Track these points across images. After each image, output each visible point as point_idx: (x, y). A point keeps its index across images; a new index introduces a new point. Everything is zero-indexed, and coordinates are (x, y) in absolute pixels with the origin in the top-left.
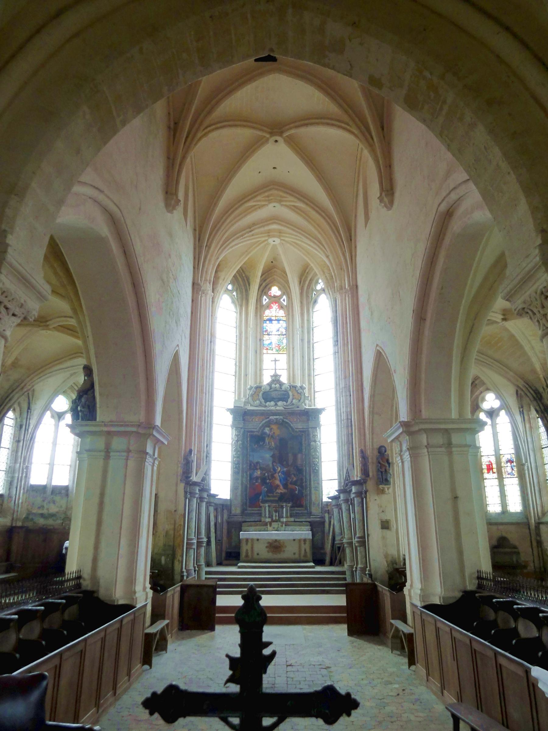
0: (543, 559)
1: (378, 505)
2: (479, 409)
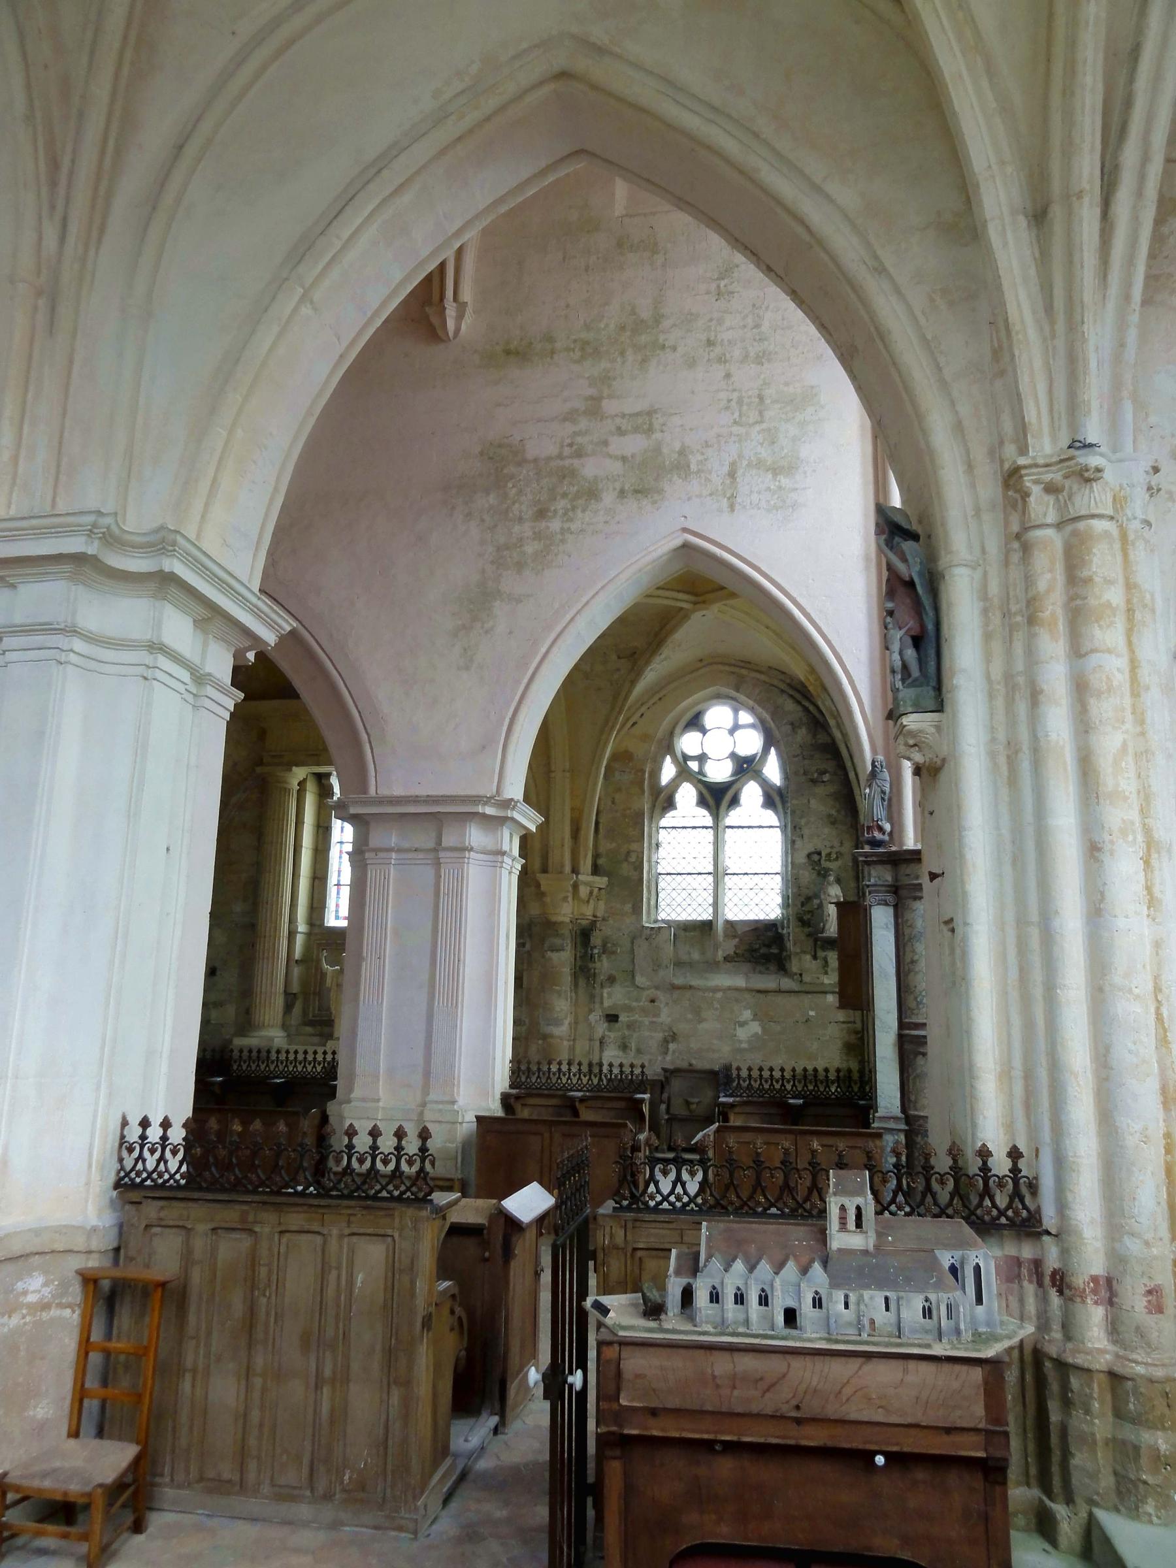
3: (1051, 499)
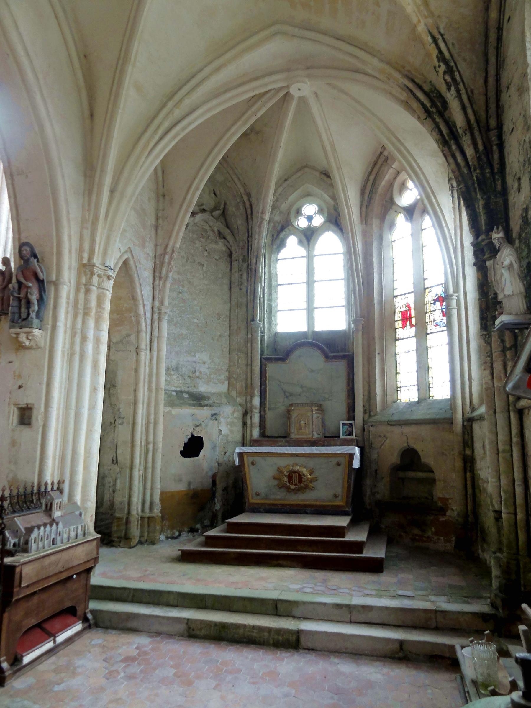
0: (474, 495)
1: (14, 372)
2: (394, 207)
3: (97, 278)
